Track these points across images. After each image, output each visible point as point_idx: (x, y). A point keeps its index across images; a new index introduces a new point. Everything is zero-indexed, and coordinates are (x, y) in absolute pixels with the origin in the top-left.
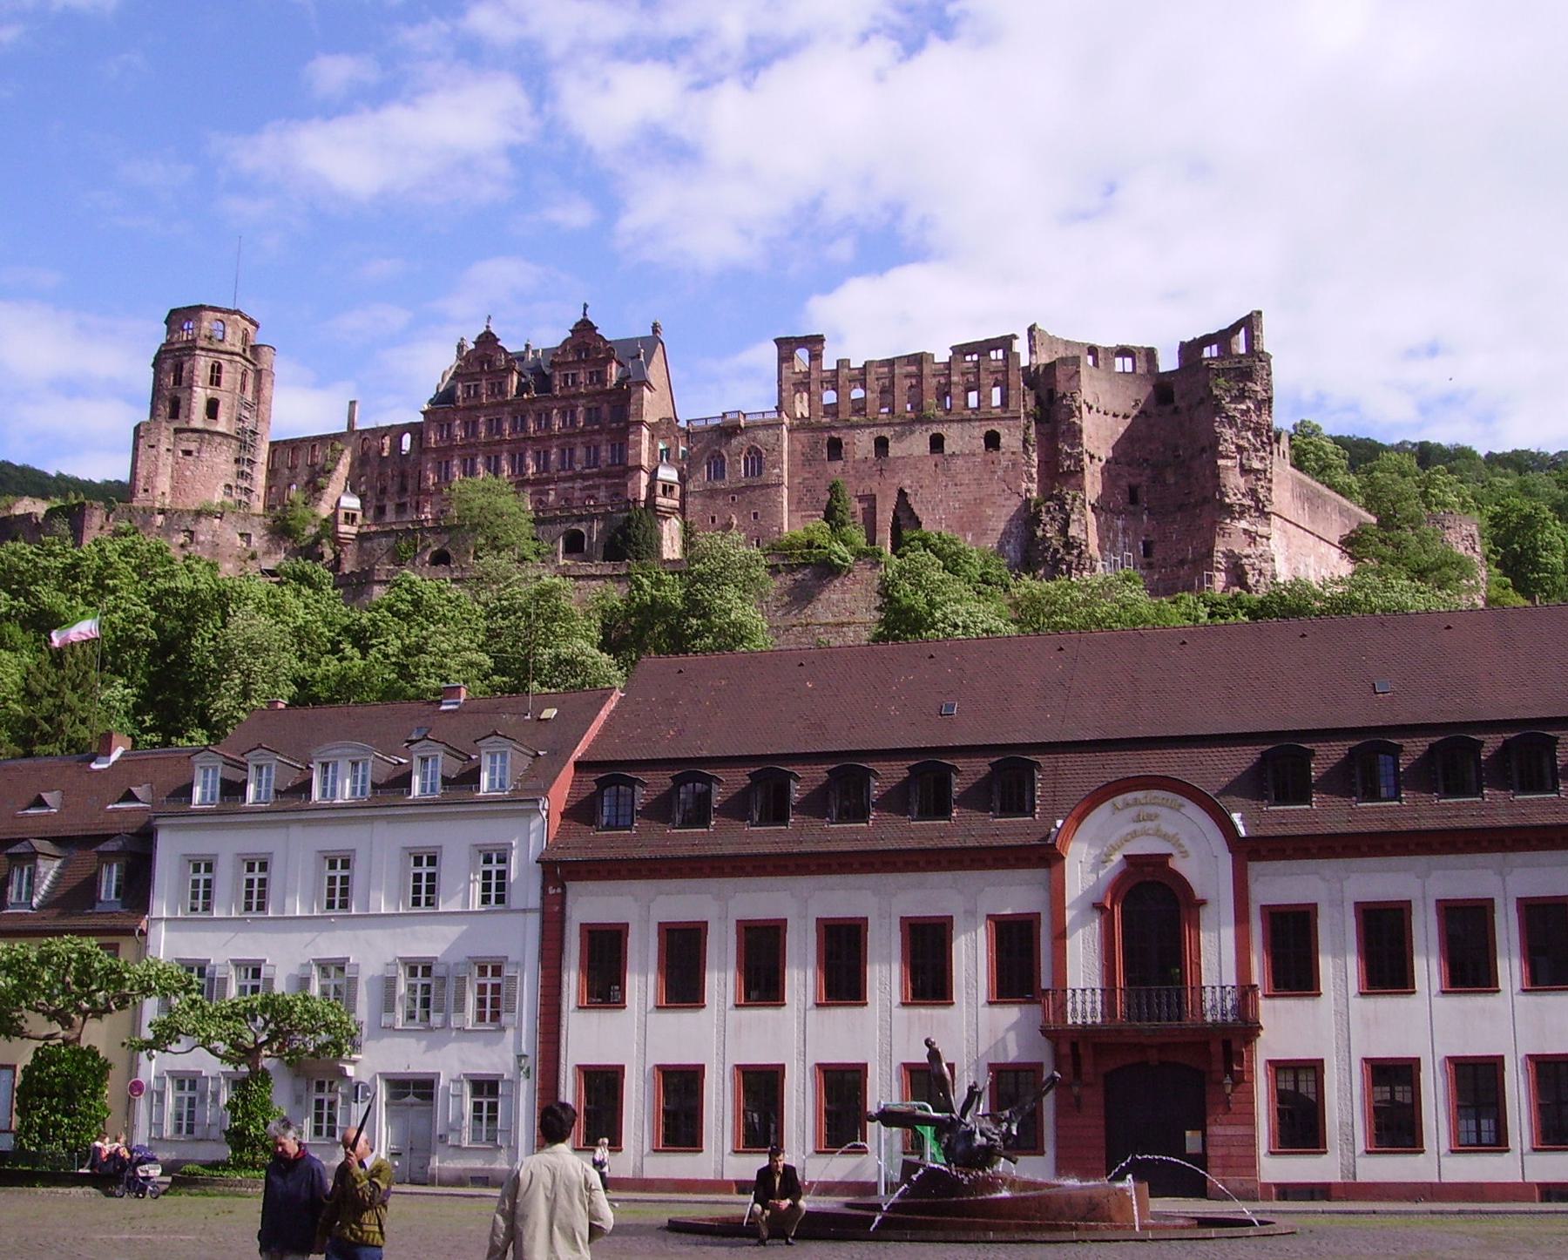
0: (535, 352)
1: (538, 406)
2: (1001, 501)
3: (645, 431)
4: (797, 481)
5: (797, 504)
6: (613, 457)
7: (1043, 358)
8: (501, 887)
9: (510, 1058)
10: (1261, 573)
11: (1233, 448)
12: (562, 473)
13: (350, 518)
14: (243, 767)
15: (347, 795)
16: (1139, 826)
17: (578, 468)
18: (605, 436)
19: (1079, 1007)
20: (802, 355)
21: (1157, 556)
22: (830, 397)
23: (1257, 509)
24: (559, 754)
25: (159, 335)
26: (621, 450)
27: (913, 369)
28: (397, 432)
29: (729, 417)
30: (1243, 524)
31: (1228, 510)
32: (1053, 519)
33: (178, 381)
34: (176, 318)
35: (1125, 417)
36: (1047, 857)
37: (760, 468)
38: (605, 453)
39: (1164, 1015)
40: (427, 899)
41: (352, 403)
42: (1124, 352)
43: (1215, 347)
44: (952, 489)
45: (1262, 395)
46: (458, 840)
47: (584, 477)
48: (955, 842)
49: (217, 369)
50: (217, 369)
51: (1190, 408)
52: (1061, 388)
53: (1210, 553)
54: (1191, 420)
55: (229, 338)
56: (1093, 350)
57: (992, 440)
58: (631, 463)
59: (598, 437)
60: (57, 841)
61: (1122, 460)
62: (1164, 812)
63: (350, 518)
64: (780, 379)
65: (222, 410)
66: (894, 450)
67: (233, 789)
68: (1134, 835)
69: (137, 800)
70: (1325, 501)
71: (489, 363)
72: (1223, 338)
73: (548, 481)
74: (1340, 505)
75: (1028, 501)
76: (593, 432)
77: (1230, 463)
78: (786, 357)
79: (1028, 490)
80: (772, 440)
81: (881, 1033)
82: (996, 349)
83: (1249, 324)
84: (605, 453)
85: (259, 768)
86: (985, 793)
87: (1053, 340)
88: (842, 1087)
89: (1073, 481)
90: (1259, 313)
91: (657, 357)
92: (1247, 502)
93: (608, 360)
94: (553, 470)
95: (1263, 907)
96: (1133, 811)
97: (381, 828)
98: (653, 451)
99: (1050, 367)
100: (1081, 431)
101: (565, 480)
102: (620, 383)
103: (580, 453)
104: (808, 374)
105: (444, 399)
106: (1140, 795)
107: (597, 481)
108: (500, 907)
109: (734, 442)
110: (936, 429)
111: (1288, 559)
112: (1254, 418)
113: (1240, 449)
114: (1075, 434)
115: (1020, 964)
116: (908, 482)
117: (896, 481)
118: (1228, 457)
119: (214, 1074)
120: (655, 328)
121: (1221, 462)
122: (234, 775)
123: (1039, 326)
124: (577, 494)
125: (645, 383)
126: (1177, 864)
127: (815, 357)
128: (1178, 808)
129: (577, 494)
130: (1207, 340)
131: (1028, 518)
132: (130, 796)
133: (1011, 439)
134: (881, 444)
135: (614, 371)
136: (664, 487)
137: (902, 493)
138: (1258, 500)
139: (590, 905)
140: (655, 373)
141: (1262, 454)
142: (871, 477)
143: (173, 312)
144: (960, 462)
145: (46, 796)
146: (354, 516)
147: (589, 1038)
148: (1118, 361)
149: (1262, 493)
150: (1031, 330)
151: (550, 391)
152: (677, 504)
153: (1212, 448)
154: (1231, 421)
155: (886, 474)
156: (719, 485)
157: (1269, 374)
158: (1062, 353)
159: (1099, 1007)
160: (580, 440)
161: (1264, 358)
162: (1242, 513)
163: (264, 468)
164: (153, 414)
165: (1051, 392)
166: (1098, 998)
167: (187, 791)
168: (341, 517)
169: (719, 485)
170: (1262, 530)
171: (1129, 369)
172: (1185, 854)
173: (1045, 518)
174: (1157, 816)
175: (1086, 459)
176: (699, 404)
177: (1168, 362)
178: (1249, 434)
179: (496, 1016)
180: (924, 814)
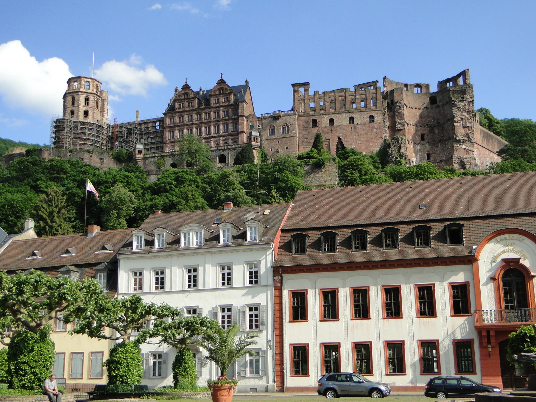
0: (203, 91)
1: (206, 111)
2: (375, 140)
4: (301, 135)
5: (302, 143)
6: (234, 129)
7: (388, 89)
8: (256, 277)
9: (265, 342)
10: (471, 164)
11: (460, 119)
13: (140, 152)
14: (153, 235)
15: (195, 244)
17: (221, 132)
18: (231, 121)
19: (489, 317)
21: (432, 158)
22: (312, 105)
23: (469, 141)
24: (275, 227)
25: (64, 88)
26: (236, 126)
27: (343, 94)
29: (276, 113)
30: (464, 147)
31: (458, 141)
32: (395, 146)
33: (73, 104)
35: (419, 109)
36: (470, 260)
37: (288, 131)
39: (524, 320)
40: (228, 283)
41: (137, 112)
42: (418, 86)
43: (451, 83)
44: (357, 137)
45: (470, 100)
47: (224, 136)
48: (434, 255)
50: (87, 100)
51: (443, 105)
52: (396, 99)
53: (452, 158)
54: (443, 109)
55: (91, 88)
56: (406, 85)
57: (372, 118)
60: (77, 266)
61: (418, 125)
63: (140, 152)
64: (294, 99)
65: (90, 113)
67: (150, 243)
68: (504, 252)
69: (106, 249)
70: (492, 138)
71: (187, 95)
72: (454, 80)
73: (210, 138)
74: (498, 139)
75: (385, 140)
76: (226, 120)
77: (458, 124)
79: (385, 136)
80: (292, 121)
81: (411, 329)
84: (231, 127)
85: (159, 235)
87: (392, 82)
88: (396, 351)
89: (401, 132)
90: (468, 70)
92: (465, 138)
93: (230, 93)
96: (505, 242)
98: (247, 126)
99: (392, 92)
100: (404, 115)
101: (216, 137)
102: (235, 102)
103: (222, 127)
106: (506, 236)
107: (228, 137)
108: (256, 285)
109: (278, 122)
111: (480, 159)
112: (467, 108)
113: (462, 119)
114: (402, 116)
115: (462, 300)
116: (341, 135)
117: (337, 134)
118: (458, 122)
119: (146, 352)
120: (247, 82)
121: (455, 124)
122: (150, 238)
123: (387, 77)
124: (221, 142)
125: (244, 101)
126: (522, 262)
127: (307, 90)
128: (522, 241)
130: (448, 80)
131: (386, 147)
132: (104, 248)
133: (378, 118)
134: (331, 121)
135: (232, 97)
136: (254, 138)
137: (339, 139)
138: (469, 138)
139: (293, 283)
140: (247, 98)
141: (470, 121)
142: (328, 133)
144: (360, 127)
145: (70, 249)
146: (141, 151)
147: (295, 333)
148: (416, 89)
149: (470, 135)
150: (384, 78)
151: (210, 105)
152: (259, 144)
153: (452, 119)
155: (334, 132)
156: (273, 137)
157: (473, 92)
158: (394, 87)
159: (493, 317)
161: (470, 86)
162: (463, 142)
165: (392, 101)
166: (493, 313)
167: (130, 245)
168: (137, 152)
169: (273, 137)
170: (471, 148)
171: (419, 91)
173: (392, 146)
175: (406, 125)
177: (434, 89)
178: (466, 114)
179: (257, 327)
180: (420, 244)
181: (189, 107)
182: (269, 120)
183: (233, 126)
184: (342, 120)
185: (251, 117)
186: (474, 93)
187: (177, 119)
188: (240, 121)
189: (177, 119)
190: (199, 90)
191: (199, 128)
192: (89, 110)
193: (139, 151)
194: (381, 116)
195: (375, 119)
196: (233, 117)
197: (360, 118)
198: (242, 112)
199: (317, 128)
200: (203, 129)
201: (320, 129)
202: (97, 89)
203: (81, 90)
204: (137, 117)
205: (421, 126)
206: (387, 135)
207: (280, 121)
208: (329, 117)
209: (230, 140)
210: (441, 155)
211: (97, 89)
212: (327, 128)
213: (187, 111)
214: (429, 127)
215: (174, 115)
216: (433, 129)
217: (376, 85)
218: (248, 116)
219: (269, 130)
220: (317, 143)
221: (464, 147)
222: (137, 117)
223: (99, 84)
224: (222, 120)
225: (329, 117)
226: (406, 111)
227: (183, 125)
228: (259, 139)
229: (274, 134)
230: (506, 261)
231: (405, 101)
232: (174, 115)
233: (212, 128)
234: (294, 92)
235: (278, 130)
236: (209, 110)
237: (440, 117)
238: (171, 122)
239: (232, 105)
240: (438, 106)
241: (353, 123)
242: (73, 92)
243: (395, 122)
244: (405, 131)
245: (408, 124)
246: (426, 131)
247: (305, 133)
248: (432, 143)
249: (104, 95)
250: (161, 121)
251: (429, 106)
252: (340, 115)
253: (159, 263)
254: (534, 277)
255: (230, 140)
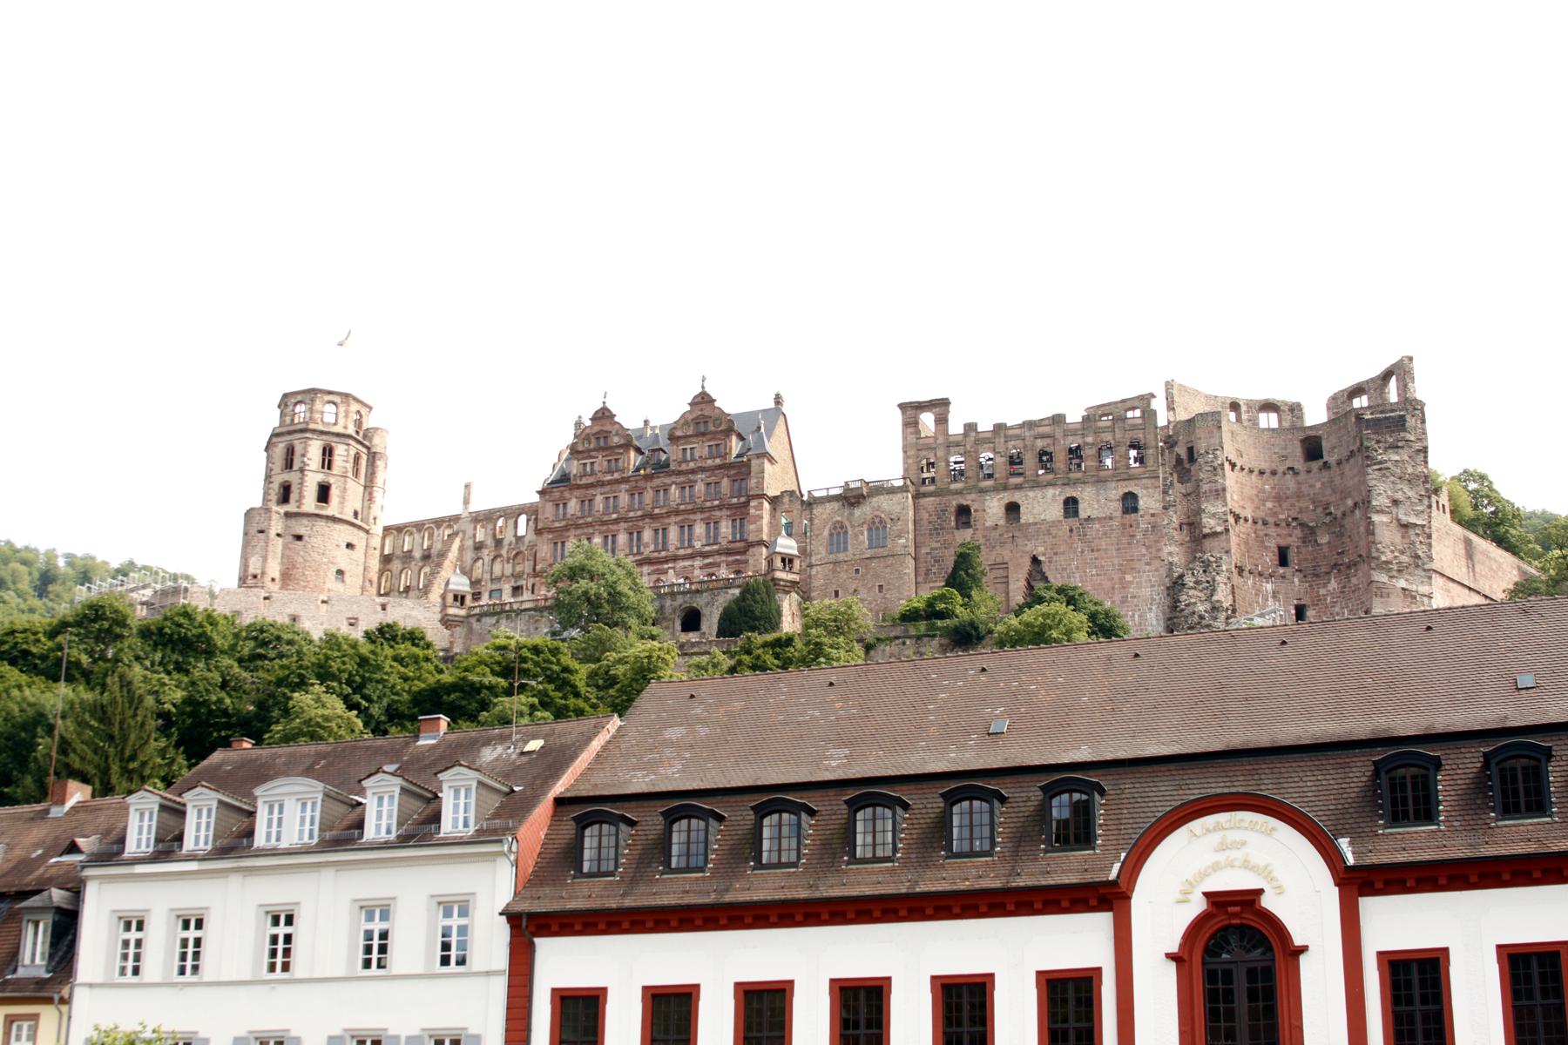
0: (653, 428)
1: (657, 482)
3: (766, 505)
6: (734, 534)
7: (1183, 415)
12: (682, 552)
16: (1221, 857)
17: (698, 545)
18: (725, 512)
20: (927, 420)
25: (273, 420)
26: (742, 526)
28: (511, 513)
29: (852, 486)
31: (1385, 566)
33: (289, 464)
34: (287, 401)
35: (1274, 473)
36: (1110, 898)
38: (725, 529)
41: (467, 486)
42: (1269, 406)
43: (1365, 398)
44: (1090, 556)
45: (1418, 446)
46: (413, 892)
47: (704, 555)
49: (328, 452)
50: (328, 452)
51: (1339, 463)
52: (1201, 447)
55: (341, 421)
56: (1235, 406)
57: (1130, 503)
58: (752, 538)
59: (718, 513)
61: (1271, 520)
62: (1253, 838)
65: (334, 493)
66: (1026, 517)
68: (1216, 867)
76: (712, 508)
77: (1385, 518)
78: (911, 424)
82: (1133, 408)
83: (1400, 371)
84: (725, 529)
86: (1056, 829)
91: (779, 429)
92: (1404, 558)
94: (672, 548)
95: (1380, 954)
96: (1215, 838)
97: (327, 877)
100: (1224, 490)
101: (685, 558)
103: (699, 529)
104: (935, 438)
105: (562, 481)
107: (717, 559)
109: (857, 512)
110: (1070, 492)
113: (1396, 502)
114: (1220, 493)
116: (1041, 549)
118: (1382, 512)
120: (778, 400)
121: (1376, 518)
123: (1179, 380)
124: (697, 572)
125: (765, 455)
126: (1267, 902)
127: (942, 421)
129: (697, 572)
130: (1357, 391)
133: (1149, 501)
134: (1013, 509)
135: (735, 446)
137: (1035, 560)
139: (564, 963)
140: (773, 446)
143: (285, 396)
146: (463, 598)
150: (1169, 386)
153: (1365, 504)
154: (1383, 470)
155: (1020, 541)
156: (841, 556)
157: (1423, 422)
158: (1199, 407)
160: (699, 516)
163: (377, 553)
164: (266, 500)
165: (1191, 450)
168: (450, 598)
169: (841, 556)
170: (1424, 589)
172: (1280, 891)
173: (1189, 580)
174: (1244, 844)
175: (1231, 520)
176: (821, 473)
181: (611, 472)
182: (830, 507)
183: (734, 527)
184: (1042, 506)
185: (786, 499)
186: (1428, 425)
187: (573, 506)
188: (752, 511)
189: (573, 506)
190: (641, 425)
191: (635, 533)
192: (332, 480)
193: (456, 598)
194: (1158, 496)
195: (1141, 502)
196: (735, 500)
197: (1093, 502)
198: (760, 484)
199: (970, 531)
200: (647, 535)
201: (979, 534)
202: (359, 423)
203: (312, 426)
204: (466, 502)
205: (1277, 525)
206: (1173, 552)
207: (863, 512)
208: (1007, 497)
209: (724, 565)
210: (1337, 609)
211: (359, 423)
212: (999, 531)
213: (602, 484)
214: (1303, 525)
215: (567, 495)
216: (1312, 531)
217: (1149, 404)
218: (776, 498)
219: (831, 535)
220: (962, 575)
221: (1402, 583)
222: (466, 502)
223: (364, 411)
224: (702, 510)
225: (1007, 497)
226: (1231, 479)
227: (589, 525)
228: (797, 563)
229: (846, 549)
230: (1217, 900)
231: (1229, 451)
232: (567, 495)
233: (673, 533)
234: (906, 425)
235: (856, 536)
236: (668, 481)
237: (1332, 499)
238: (557, 515)
239: (730, 466)
240: (1326, 466)
241: (1076, 514)
242: (290, 433)
243: (1199, 511)
244: (1228, 541)
245: (1237, 518)
246: (1293, 539)
247: (934, 545)
248: (1314, 575)
249: (377, 440)
250: (531, 511)
251: (1299, 464)
252: (1038, 493)
253: (191, 896)
254: (1304, 949)
255: (724, 565)
